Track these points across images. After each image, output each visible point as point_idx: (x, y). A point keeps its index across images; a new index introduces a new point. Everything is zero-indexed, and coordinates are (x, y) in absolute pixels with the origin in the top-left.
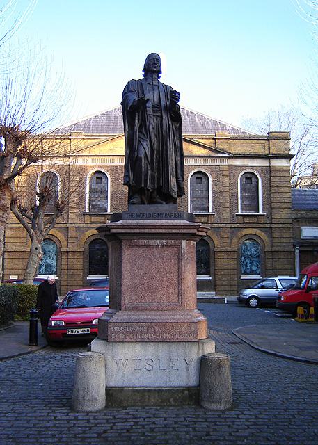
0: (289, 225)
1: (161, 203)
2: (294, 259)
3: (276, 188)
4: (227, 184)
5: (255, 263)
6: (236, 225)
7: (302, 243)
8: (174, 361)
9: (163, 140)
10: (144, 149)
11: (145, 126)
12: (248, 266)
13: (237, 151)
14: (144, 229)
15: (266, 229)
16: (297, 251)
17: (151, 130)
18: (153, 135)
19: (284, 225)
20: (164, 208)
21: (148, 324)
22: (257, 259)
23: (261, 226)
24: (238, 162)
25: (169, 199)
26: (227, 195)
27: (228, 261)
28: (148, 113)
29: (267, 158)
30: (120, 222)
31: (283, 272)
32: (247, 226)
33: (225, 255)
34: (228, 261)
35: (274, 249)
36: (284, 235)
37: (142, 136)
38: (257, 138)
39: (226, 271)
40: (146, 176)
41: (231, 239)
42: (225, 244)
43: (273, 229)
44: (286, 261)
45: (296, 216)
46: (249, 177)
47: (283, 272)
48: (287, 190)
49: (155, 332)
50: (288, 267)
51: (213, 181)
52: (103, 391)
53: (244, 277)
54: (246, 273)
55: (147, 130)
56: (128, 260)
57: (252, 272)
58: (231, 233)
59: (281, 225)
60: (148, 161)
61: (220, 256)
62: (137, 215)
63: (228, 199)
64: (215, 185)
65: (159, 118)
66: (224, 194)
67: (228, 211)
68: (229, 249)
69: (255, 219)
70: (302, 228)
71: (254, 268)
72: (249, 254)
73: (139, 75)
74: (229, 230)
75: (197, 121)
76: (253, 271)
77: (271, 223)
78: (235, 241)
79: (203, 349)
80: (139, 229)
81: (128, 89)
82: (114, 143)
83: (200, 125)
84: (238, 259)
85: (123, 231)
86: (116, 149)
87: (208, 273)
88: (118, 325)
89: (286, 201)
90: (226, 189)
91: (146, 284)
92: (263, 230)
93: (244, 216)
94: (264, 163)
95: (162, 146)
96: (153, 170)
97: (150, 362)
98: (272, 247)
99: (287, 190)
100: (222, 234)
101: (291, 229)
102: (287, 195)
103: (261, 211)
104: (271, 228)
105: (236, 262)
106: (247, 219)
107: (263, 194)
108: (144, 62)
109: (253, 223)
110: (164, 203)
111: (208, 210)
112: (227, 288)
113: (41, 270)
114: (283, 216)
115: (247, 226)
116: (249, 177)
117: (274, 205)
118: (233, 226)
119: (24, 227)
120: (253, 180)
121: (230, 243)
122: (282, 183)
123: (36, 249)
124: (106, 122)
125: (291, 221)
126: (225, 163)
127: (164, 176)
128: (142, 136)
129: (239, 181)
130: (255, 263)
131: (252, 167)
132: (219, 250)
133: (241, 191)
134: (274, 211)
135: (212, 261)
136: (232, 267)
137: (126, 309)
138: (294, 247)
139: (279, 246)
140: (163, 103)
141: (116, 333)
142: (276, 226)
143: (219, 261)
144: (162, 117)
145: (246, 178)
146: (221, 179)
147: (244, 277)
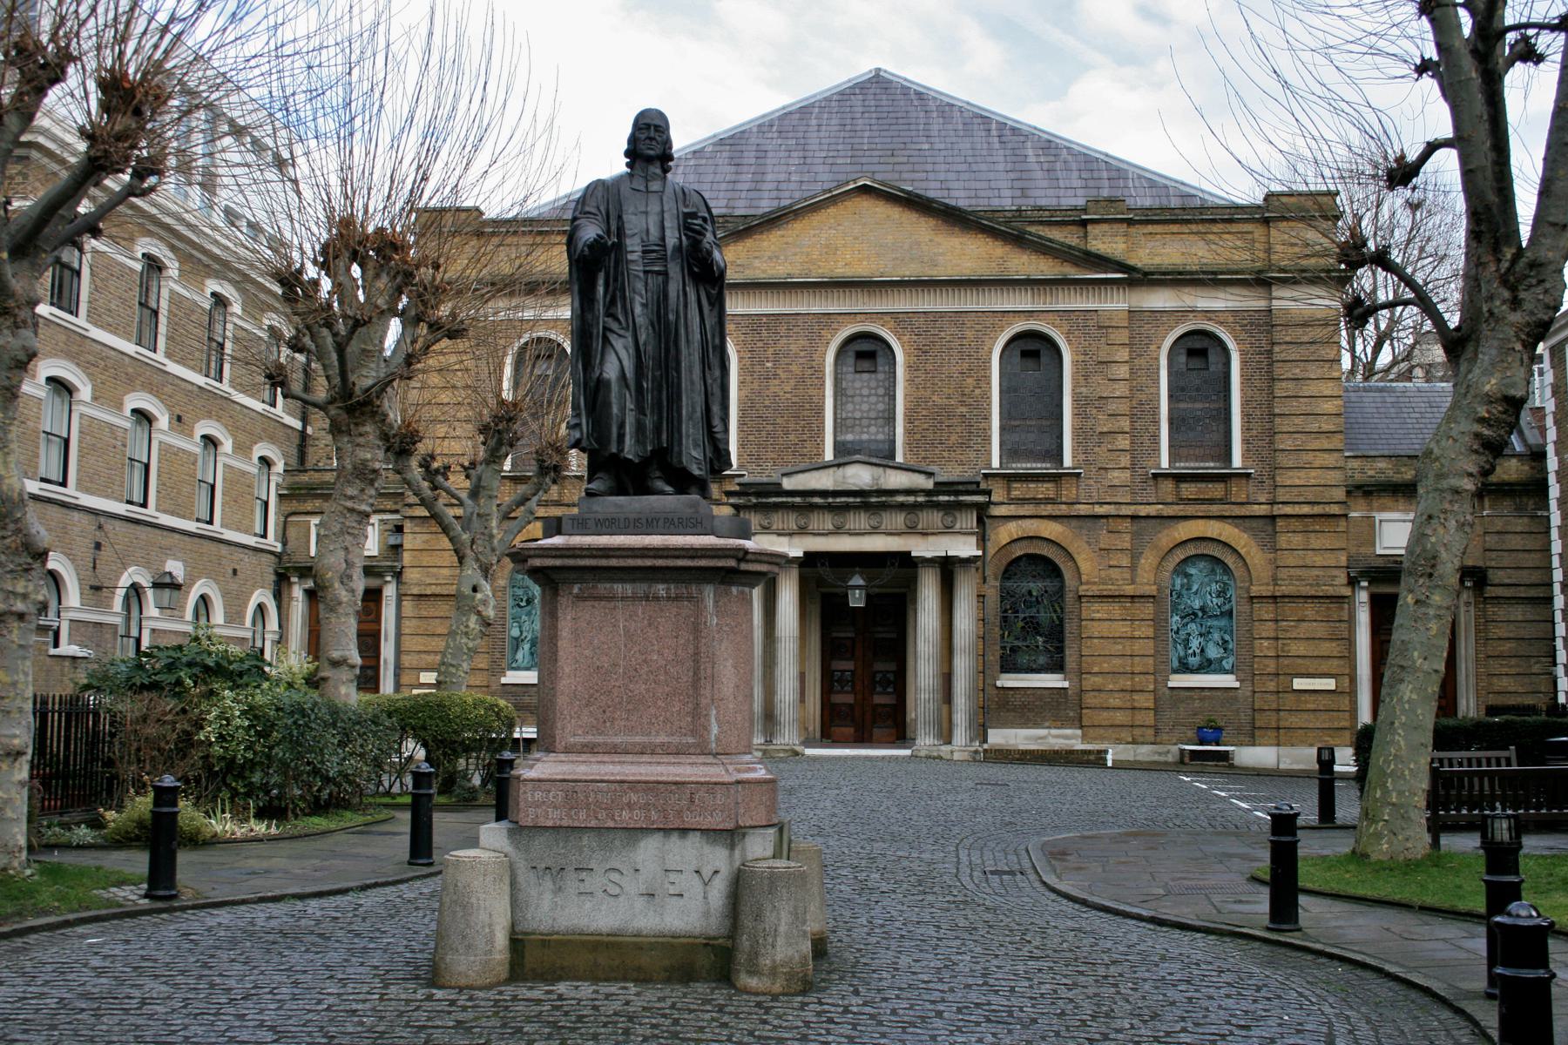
0: (1335, 509)
1: (662, 493)
2: (1351, 621)
3: (1291, 385)
4: (1123, 371)
5: (1216, 636)
6: (1152, 510)
7: (1378, 570)
8: (672, 877)
9: (666, 332)
10: (616, 363)
11: (624, 298)
12: (1195, 644)
13: (1157, 260)
14: (608, 557)
15: (1255, 523)
16: (1363, 596)
17: (638, 310)
18: (640, 320)
19: (1317, 510)
20: (667, 501)
21: (612, 786)
22: (1223, 622)
23: (1237, 511)
24: (1160, 300)
25: (683, 482)
26: (1124, 407)
27: (1122, 629)
28: (632, 267)
29: (1261, 281)
30: (557, 540)
31: (1312, 666)
32: (1190, 510)
33: (1115, 609)
34: (1122, 629)
35: (1284, 589)
36: (1316, 541)
37: (614, 326)
38: (1229, 216)
39: (1117, 661)
40: (622, 426)
41: (1135, 556)
42: (1115, 573)
43: (1280, 523)
44: (1321, 630)
45: (1358, 478)
46: (1199, 349)
47: (1312, 666)
48: (1328, 389)
49: (630, 806)
50: (1327, 648)
51: (1075, 363)
52: (501, 940)
53: (1178, 681)
54: (1185, 668)
55: (628, 312)
56: (576, 633)
57: (1207, 666)
58: (1135, 535)
59: (1306, 510)
60: (627, 387)
61: (1098, 610)
62: (598, 522)
63: (1125, 424)
64: (1083, 375)
65: (660, 278)
66: (1112, 407)
67: (1125, 460)
68: (1129, 590)
69: (1216, 490)
70: (1378, 516)
71: (1213, 652)
72: (1197, 604)
73: (614, 164)
74: (1127, 524)
75: (1032, 159)
76: (1210, 662)
77: (1272, 503)
78: (1148, 561)
79: (744, 849)
80: (595, 557)
81: (584, 204)
82: (749, 243)
83: (1039, 174)
84: (1158, 622)
85: (558, 562)
86: (757, 263)
87: (1057, 667)
88: (544, 786)
89: (1325, 427)
90: (1121, 389)
91: (615, 691)
92: (1248, 523)
93: (1179, 478)
94: (1249, 301)
95: (667, 350)
96: (640, 409)
97: (615, 876)
98: (1275, 580)
99: (1328, 389)
100: (1105, 540)
101: (1343, 523)
102: (1329, 407)
103: (1237, 461)
104: (1273, 518)
105: (1150, 632)
106: (1189, 490)
107: (1245, 403)
108: (627, 130)
109: (1211, 501)
110: (668, 489)
111: (1058, 456)
112: (1120, 717)
113: (519, 656)
114: (1314, 477)
115: (1190, 510)
116: (1199, 349)
117: (1285, 443)
118: (1143, 511)
119: (432, 516)
120: (1213, 357)
121: (1133, 568)
122: (1312, 366)
123: (475, 589)
124: (727, 171)
125: (1340, 494)
126: (1116, 303)
127: (670, 421)
128: (614, 326)
129: (1164, 362)
130: (1216, 636)
131: (1208, 314)
132: (1094, 590)
133: (1170, 397)
134: (1282, 459)
135: (1069, 627)
136: (1138, 647)
137: (567, 751)
138: (1352, 582)
139: (1300, 578)
140: (671, 241)
141: (537, 805)
142: (1288, 510)
143: (1095, 629)
144: (665, 274)
145: (1191, 353)
146: (1103, 356)
147: (1178, 681)
